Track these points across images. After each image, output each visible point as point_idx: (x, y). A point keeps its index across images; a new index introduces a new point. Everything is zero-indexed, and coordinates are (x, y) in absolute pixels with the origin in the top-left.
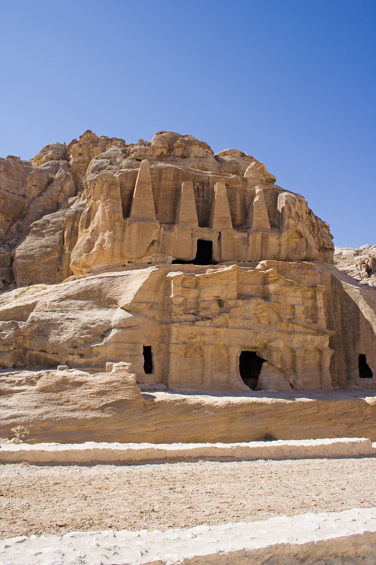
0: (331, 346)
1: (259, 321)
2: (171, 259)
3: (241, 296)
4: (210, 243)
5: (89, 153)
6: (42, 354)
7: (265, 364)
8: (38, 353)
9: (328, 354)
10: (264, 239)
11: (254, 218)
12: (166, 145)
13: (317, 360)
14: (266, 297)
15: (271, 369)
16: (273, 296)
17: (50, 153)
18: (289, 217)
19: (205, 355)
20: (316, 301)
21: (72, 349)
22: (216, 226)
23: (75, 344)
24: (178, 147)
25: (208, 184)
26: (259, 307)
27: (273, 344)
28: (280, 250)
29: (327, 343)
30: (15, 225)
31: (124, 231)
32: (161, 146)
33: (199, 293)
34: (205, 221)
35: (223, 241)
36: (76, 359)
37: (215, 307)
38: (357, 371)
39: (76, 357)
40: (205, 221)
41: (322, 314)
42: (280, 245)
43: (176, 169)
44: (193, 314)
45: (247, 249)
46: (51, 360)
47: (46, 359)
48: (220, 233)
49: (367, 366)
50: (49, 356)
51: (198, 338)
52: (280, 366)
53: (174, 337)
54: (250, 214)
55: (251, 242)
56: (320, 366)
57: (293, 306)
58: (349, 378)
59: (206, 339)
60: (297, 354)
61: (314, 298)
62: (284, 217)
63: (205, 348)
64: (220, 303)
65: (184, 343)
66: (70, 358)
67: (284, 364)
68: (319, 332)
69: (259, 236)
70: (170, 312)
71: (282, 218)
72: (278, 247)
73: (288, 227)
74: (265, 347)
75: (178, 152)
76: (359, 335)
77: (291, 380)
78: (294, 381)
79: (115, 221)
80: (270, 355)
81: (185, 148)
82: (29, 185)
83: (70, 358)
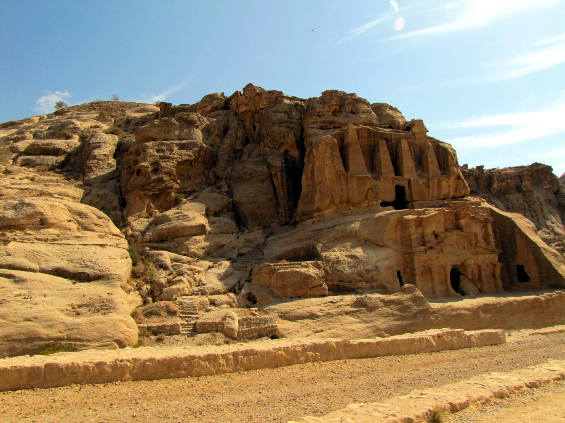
0: (500, 260)
1: (459, 247)
2: (380, 201)
3: (446, 230)
4: (403, 188)
5: (254, 104)
6: (341, 283)
7: (461, 277)
8: (338, 283)
9: (499, 265)
10: (439, 182)
11: (430, 167)
12: (339, 103)
13: (491, 271)
14: (459, 227)
15: (466, 280)
16: (464, 228)
17: (215, 103)
18: (453, 165)
19: (433, 274)
20: (487, 229)
21: (360, 278)
22: (406, 176)
23: (361, 274)
24: (348, 104)
25: (391, 140)
26: (458, 236)
27: (468, 262)
28: (449, 190)
29: (497, 259)
30: (211, 172)
31: (347, 182)
32: (335, 103)
33: (423, 230)
34: (398, 171)
35: (413, 187)
36: (364, 284)
37: (433, 238)
38: (516, 278)
39: (363, 283)
40: (398, 171)
41: (492, 239)
42: (449, 187)
43: (368, 129)
44: (422, 245)
45: (429, 191)
46: (347, 287)
47: (344, 286)
48: (409, 180)
49: (525, 273)
50: (346, 285)
51: (429, 261)
52: (471, 277)
53: (416, 263)
54: (425, 163)
55: (431, 186)
56: (494, 275)
57: (476, 235)
58: (511, 282)
59: (433, 262)
60: (482, 268)
61: (485, 227)
62: (449, 164)
63: (433, 269)
64: (436, 236)
65: (422, 266)
66: (360, 284)
67: (473, 277)
68: (493, 251)
69: (436, 182)
70: (411, 246)
71: (448, 166)
72: (447, 189)
73: (454, 174)
74: (463, 265)
75: (349, 108)
76: (517, 252)
77: (479, 287)
78: (481, 287)
79: (340, 175)
80: (465, 270)
81: (354, 106)
82: (214, 136)
83: (360, 284)
